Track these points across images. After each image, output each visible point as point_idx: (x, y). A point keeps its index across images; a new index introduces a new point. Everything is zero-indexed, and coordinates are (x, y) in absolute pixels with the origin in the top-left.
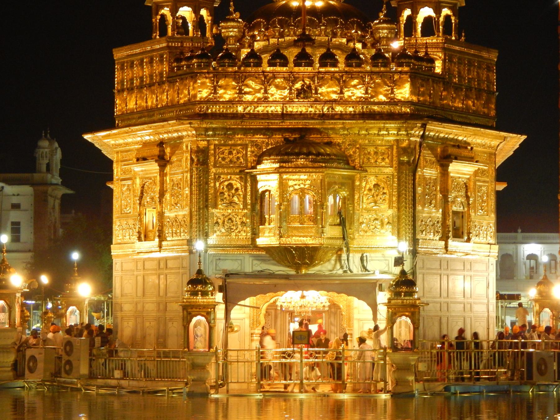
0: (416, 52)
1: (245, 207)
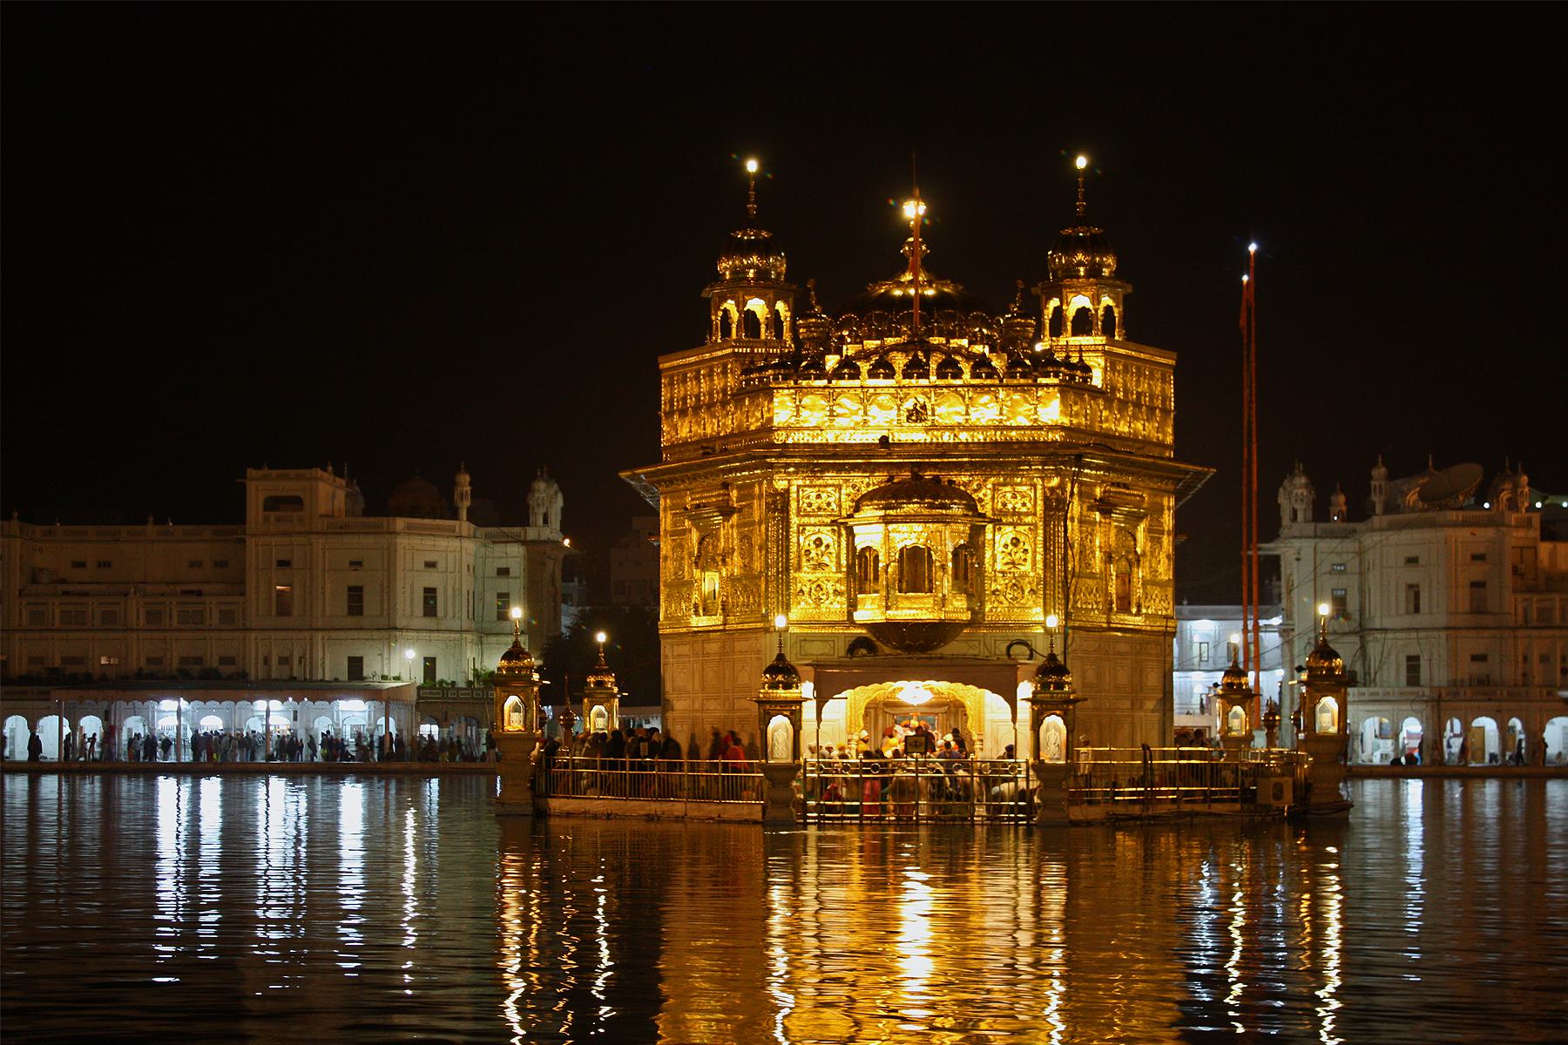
1: (839, 571)
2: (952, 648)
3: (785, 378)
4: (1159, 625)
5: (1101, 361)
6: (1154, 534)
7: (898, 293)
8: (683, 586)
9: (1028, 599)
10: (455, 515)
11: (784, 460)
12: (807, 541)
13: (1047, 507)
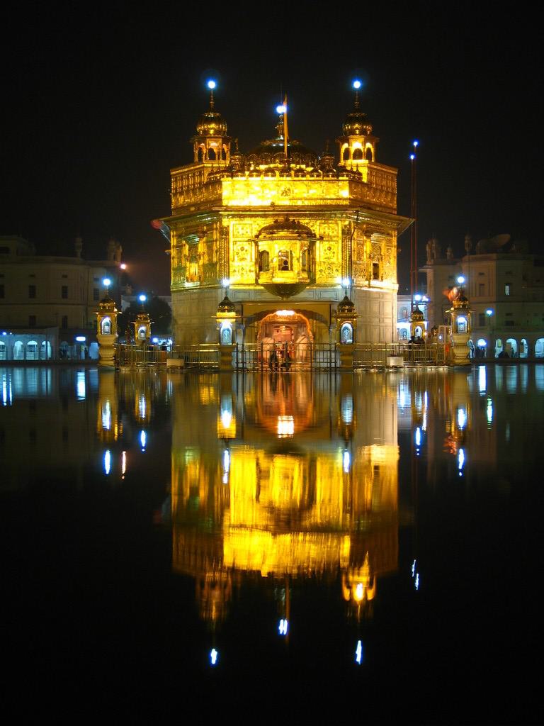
0: (352, 169)
1: (251, 261)
3: (228, 176)
8: (181, 270)
9: (335, 273)
10: (74, 255)
11: (227, 213)
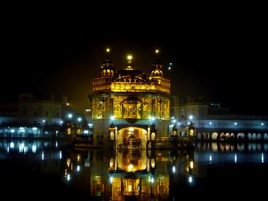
1: (121, 110)
2: (138, 123)
4: (168, 120)
5: (160, 80)
6: (167, 106)
7: (127, 69)
12: (116, 106)
13: (152, 102)
